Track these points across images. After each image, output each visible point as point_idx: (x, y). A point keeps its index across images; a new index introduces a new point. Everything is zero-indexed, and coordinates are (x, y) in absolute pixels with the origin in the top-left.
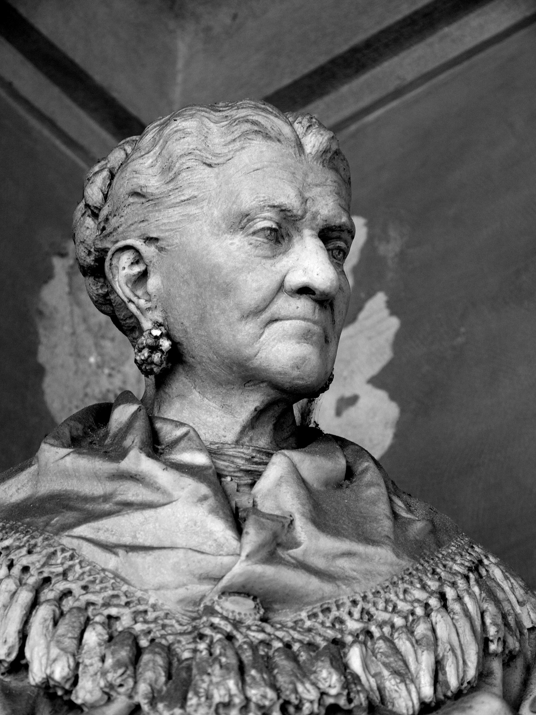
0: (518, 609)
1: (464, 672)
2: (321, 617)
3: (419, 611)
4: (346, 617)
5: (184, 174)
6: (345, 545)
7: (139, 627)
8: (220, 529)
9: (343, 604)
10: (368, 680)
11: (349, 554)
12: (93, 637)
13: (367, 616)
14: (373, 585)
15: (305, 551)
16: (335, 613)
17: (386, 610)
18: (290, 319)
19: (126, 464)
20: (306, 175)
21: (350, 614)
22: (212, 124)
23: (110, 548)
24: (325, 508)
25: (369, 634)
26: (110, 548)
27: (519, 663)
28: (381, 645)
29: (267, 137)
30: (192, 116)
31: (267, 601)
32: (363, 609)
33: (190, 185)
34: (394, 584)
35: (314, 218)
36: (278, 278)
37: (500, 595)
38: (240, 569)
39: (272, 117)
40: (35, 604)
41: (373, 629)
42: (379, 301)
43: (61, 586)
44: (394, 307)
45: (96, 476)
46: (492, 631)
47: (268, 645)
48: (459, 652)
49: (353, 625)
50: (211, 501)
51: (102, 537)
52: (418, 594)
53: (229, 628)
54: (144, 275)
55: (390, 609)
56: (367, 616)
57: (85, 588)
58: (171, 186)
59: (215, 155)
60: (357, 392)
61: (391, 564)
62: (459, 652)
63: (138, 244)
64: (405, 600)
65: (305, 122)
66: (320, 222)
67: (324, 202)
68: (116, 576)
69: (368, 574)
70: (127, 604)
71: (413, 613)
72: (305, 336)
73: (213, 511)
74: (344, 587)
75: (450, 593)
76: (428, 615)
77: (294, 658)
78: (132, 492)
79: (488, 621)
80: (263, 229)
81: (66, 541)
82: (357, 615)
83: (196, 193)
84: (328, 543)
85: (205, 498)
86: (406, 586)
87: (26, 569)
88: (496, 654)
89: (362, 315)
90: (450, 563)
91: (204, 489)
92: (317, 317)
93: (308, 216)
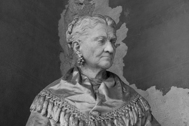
0: (145, 107)
1: (134, 122)
2: (110, 114)
3: (127, 112)
4: (114, 114)
6: (114, 100)
7: (79, 117)
8: (92, 98)
11: (115, 102)
12: (71, 118)
13: (118, 113)
14: (119, 107)
15: (107, 102)
17: (121, 112)
19: (76, 86)
20: (108, 29)
21: (115, 113)
22: (91, 20)
23: (73, 101)
24: (111, 92)
25: (118, 116)
26: (73, 101)
27: (145, 118)
28: (120, 119)
29: (101, 23)
30: (87, 18)
31: (100, 112)
33: (87, 32)
34: (122, 106)
35: (109, 38)
36: (103, 49)
37: (142, 105)
38: (96, 107)
40: (61, 111)
41: (119, 116)
42: (124, 24)
43: (65, 108)
44: (127, 26)
45: (71, 87)
46: (140, 113)
47: (101, 121)
48: (133, 119)
49: (115, 115)
50: (91, 93)
51: (72, 99)
52: (127, 108)
53: (93, 118)
54: (79, 47)
56: (118, 113)
57: (69, 109)
58: (83, 32)
59: (92, 26)
60: (120, 43)
61: (122, 103)
62: (133, 119)
63: (78, 41)
64: (124, 110)
65: (108, 19)
66: (110, 38)
68: (75, 107)
69: (118, 105)
70: (77, 112)
71: (126, 112)
72: (108, 60)
73: (91, 95)
75: (132, 107)
76: (128, 112)
77: (105, 123)
78: (77, 91)
79: (139, 111)
80: (100, 41)
81: (66, 99)
82: (116, 113)
84: (111, 100)
85: (90, 93)
87: (59, 104)
88: (140, 117)
89: (121, 27)
90: (133, 101)
91: (90, 91)
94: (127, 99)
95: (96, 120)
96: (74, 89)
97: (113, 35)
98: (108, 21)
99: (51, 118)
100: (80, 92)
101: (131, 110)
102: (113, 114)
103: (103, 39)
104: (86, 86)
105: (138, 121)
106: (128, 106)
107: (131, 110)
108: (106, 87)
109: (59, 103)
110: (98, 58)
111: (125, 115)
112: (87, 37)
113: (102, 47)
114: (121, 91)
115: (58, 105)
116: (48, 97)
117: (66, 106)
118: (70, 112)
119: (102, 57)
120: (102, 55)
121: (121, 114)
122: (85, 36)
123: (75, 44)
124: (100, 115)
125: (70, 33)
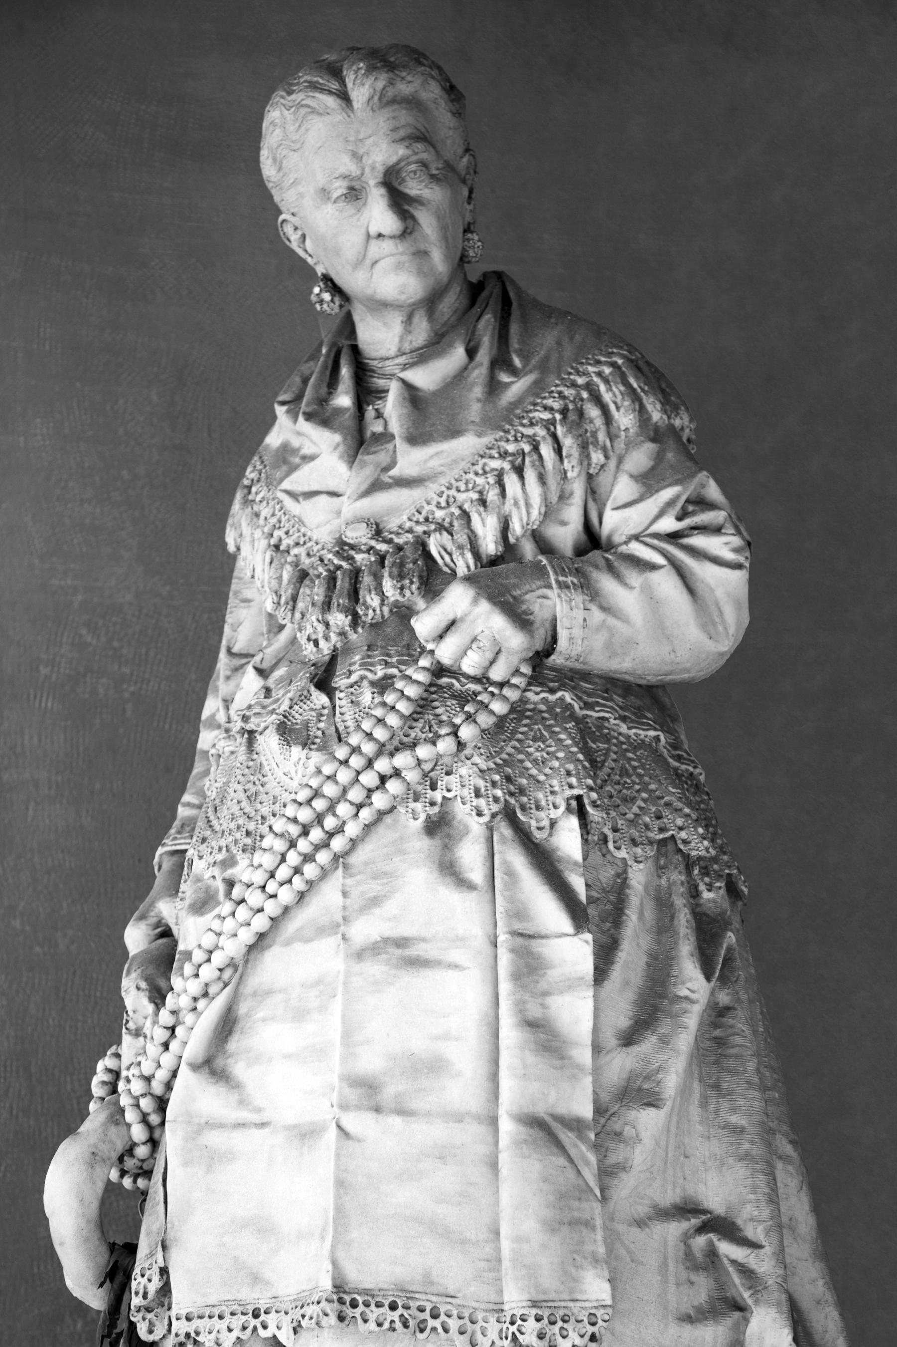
4: (435, 509)
5: (284, 162)
9: (432, 498)
10: (442, 558)
11: (437, 454)
14: (457, 472)
16: (427, 508)
18: (383, 258)
29: (320, 114)
32: (448, 496)
35: (373, 168)
36: (363, 231)
39: (317, 95)
50: (341, 448)
52: (496, 464)
55: (470, 486)
59: (293, 142)
62: (522, 503)
66: (381, 169)
67: (378, 149)
72: (399, 266)
73: (341, 457)
74: (431, 485)
82: (443, 504)
83: (296, 176)
86: (484, 460)
92: (401, 249)
93: (367, 170)
94: (501, 420)
97: (384, 146)
98: (353, 89)
111: (483, 502)
112: (300, 194)
113: (358, 220)
114: (478, 391)
121: (465, 501)
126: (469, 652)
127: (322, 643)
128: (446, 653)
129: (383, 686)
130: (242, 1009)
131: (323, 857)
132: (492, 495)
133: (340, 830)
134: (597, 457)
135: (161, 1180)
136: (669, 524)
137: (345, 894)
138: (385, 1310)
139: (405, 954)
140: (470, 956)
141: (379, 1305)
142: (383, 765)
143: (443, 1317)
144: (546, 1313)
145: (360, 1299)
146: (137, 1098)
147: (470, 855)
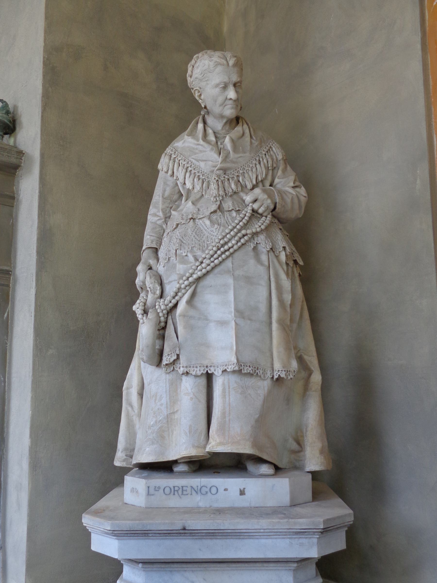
0: (277, 156)
3: (254, 166)
7: (203, 177)
16: (238, 170)
23: (198, 161)
25: (244, 172)
29: (221, 65)
34: (249, 161)
46: (269, 165)
47: (225, 180)
49: (241, 172)
52: (254, 162)
54: (201, 95)
57: (194, 169)
66: (233, 82)
72: (232, 108)
73: (215, 152)
75: (261, 160)
76: (256, 166)
79: (269, 163)
87: (184, 165)
95: (220, 181)
96: (197, 146)
99: (177, 179)
100: (204, 149)
101: (260, 163)
102: (239, 171)
103: (225, 85)
104: (209, 142)
105: (266, 175)
106: (256, 160)
107: (260, 163)
108: (232, 141)
109: (183, 163)
110: (221, 108)
111: (252, 171)
114: (249, 143)
115: (182, 165)
116: (173, 156)
117: (191, 166)
118: (195, 173)
119: (225, 106)
120: (225, 103)
122: (205, 82)
123: (196, 92)
124: (225, 174)
125: (191, 77)
126: (262, 208)
127: (218, 199)
128: (256, 206)
129: (238, 211)
130: (199, 290)
131: (227, 253)
132: (254, 170)
133: (232, 247)
134: (275, 165)
135: (174, 332)
136: (292, 184)
137: (232, 264)
138: (248, 367)
139: (249, 280)
140: (264, 283)
141: (246, 366)
142: (243, 232)
143: (259, 370)
144: (286, 370)
145: (243, 365)
146: (163, 310)
147: (264, 258)
